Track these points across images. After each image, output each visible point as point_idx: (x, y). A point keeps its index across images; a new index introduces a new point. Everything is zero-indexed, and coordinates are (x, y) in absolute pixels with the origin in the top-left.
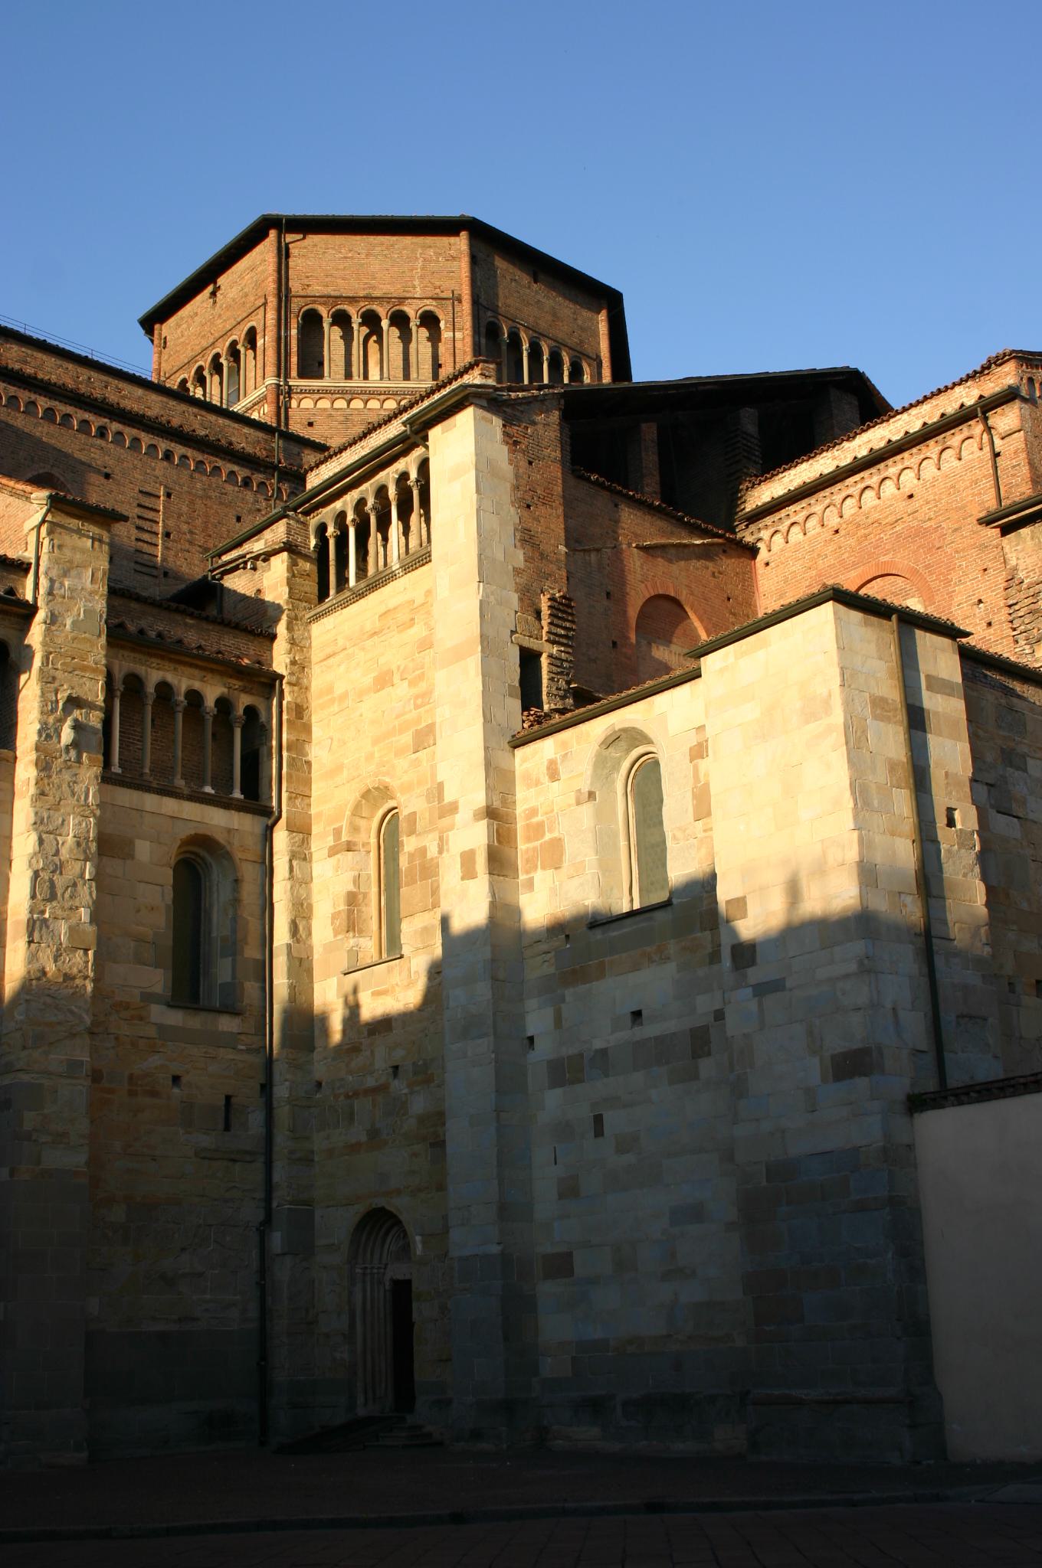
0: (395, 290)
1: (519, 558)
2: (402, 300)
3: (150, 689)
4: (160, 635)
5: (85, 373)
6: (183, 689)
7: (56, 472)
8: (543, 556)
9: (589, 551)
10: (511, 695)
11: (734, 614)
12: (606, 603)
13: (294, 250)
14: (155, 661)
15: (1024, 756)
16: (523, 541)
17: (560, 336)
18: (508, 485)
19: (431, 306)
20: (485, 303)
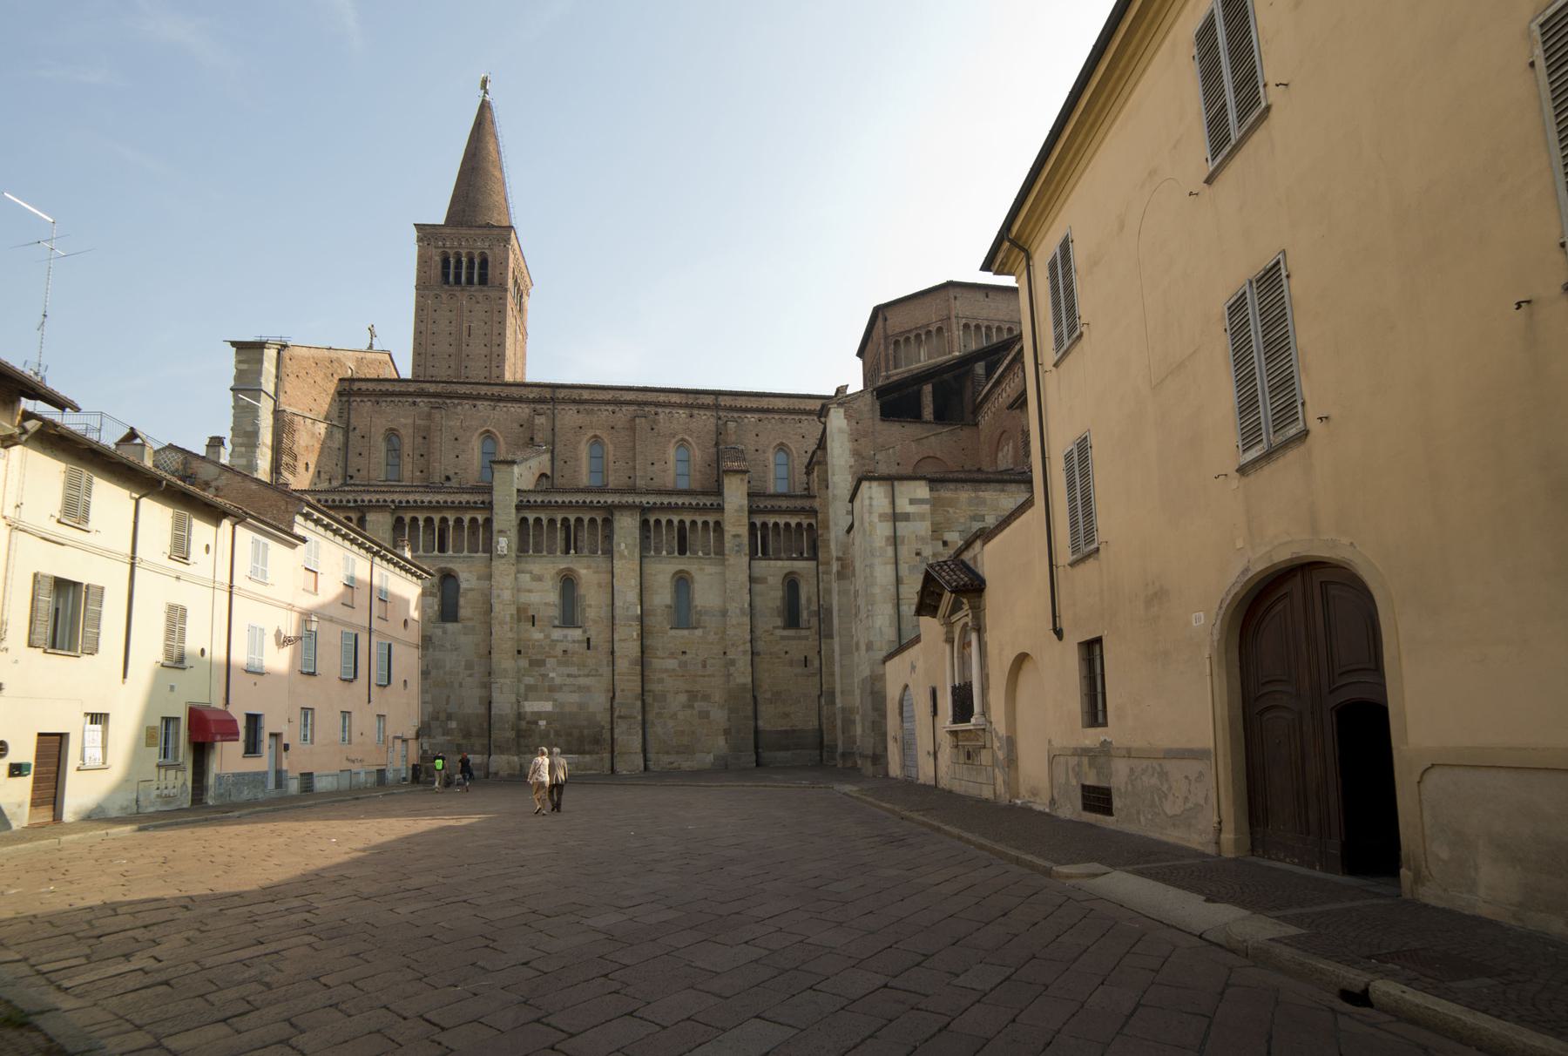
0: (925, 322)
1: (852, 461)
2: (928, 325)
3: (771, 525)
4: (772, 507)
5: (792, 400)
6: (783, 522)
7: (784, 441)
8: (863, 458)
9: (889, 449)
10: (847, 514)
11: (966, 455)
12: (897, 467)
13: (888, 317)
14: (771, 516)
15: (983, 516)
16: (854, 454)
17: (1001, 317)
18: (846, 435)
19: (939, 324)
20: (960, 315)
